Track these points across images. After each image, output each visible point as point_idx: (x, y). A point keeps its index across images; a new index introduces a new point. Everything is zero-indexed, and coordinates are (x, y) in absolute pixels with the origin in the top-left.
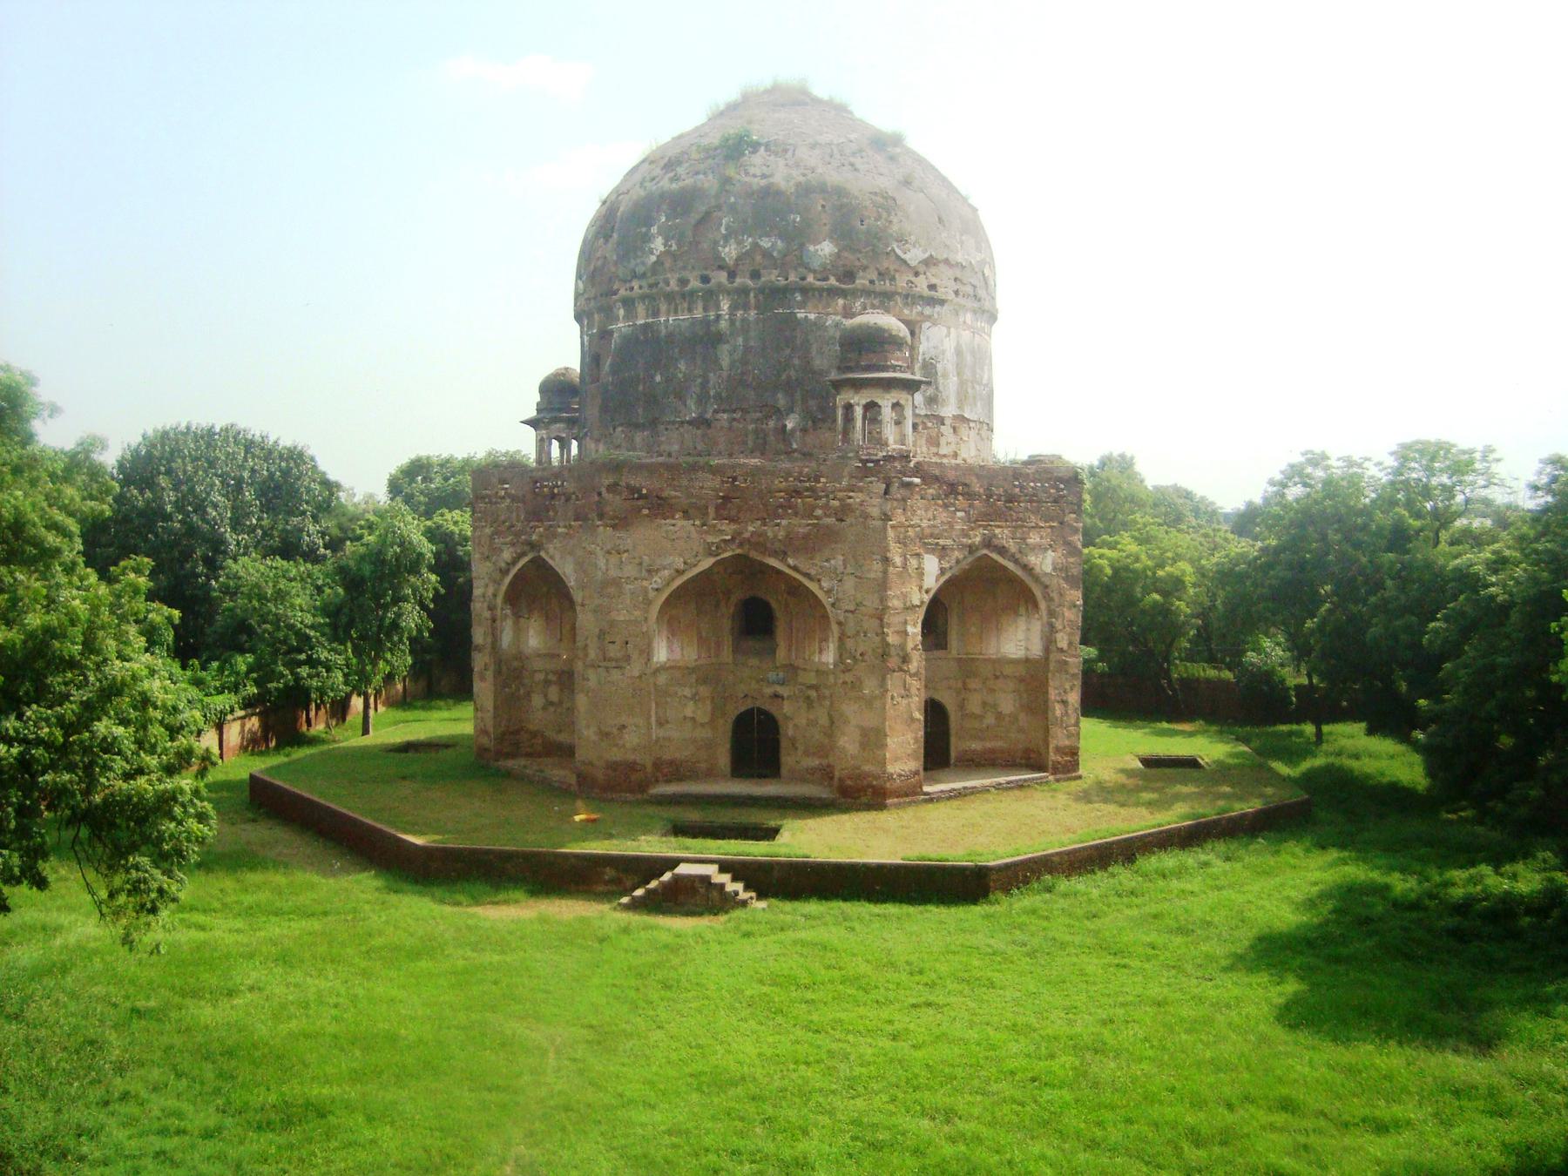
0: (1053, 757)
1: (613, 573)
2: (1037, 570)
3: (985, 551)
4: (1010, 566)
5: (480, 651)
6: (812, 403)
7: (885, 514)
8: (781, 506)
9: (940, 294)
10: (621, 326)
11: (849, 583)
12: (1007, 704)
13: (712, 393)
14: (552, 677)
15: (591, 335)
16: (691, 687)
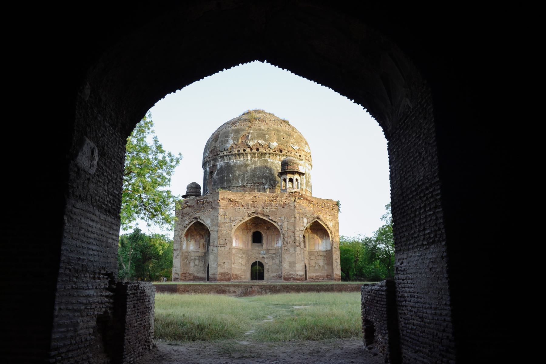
0: (335, 276)
1: (223, 221)
2: (329, 226)
3: (317, 220)
4: (323, 224)
5: (176, 251)
6: (272, 182)
7: (295, 206)
8: (268, 204)
9: (301, 158)
10: (220, 164)
11: (286, 223)
12: (321, 263)
13: (246, 179)
14: (196, 258)
15: (210, 168)
16: (241, 254)
